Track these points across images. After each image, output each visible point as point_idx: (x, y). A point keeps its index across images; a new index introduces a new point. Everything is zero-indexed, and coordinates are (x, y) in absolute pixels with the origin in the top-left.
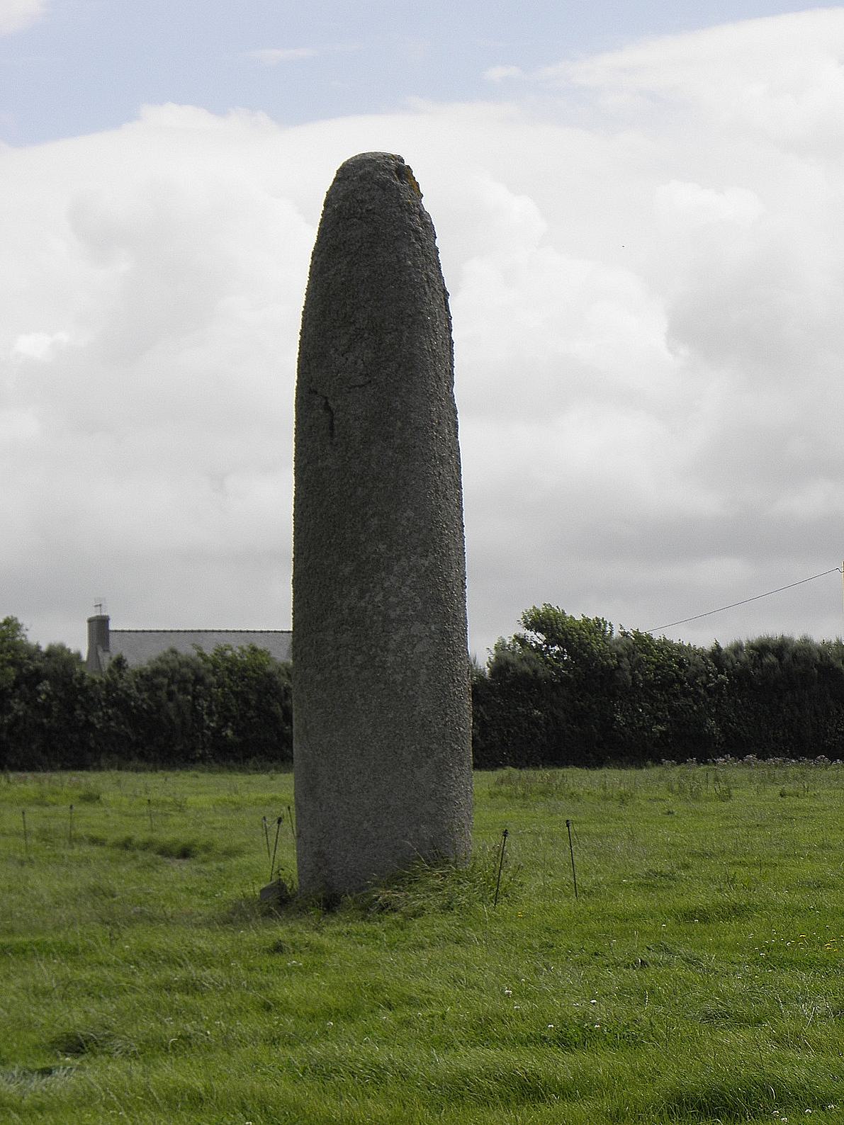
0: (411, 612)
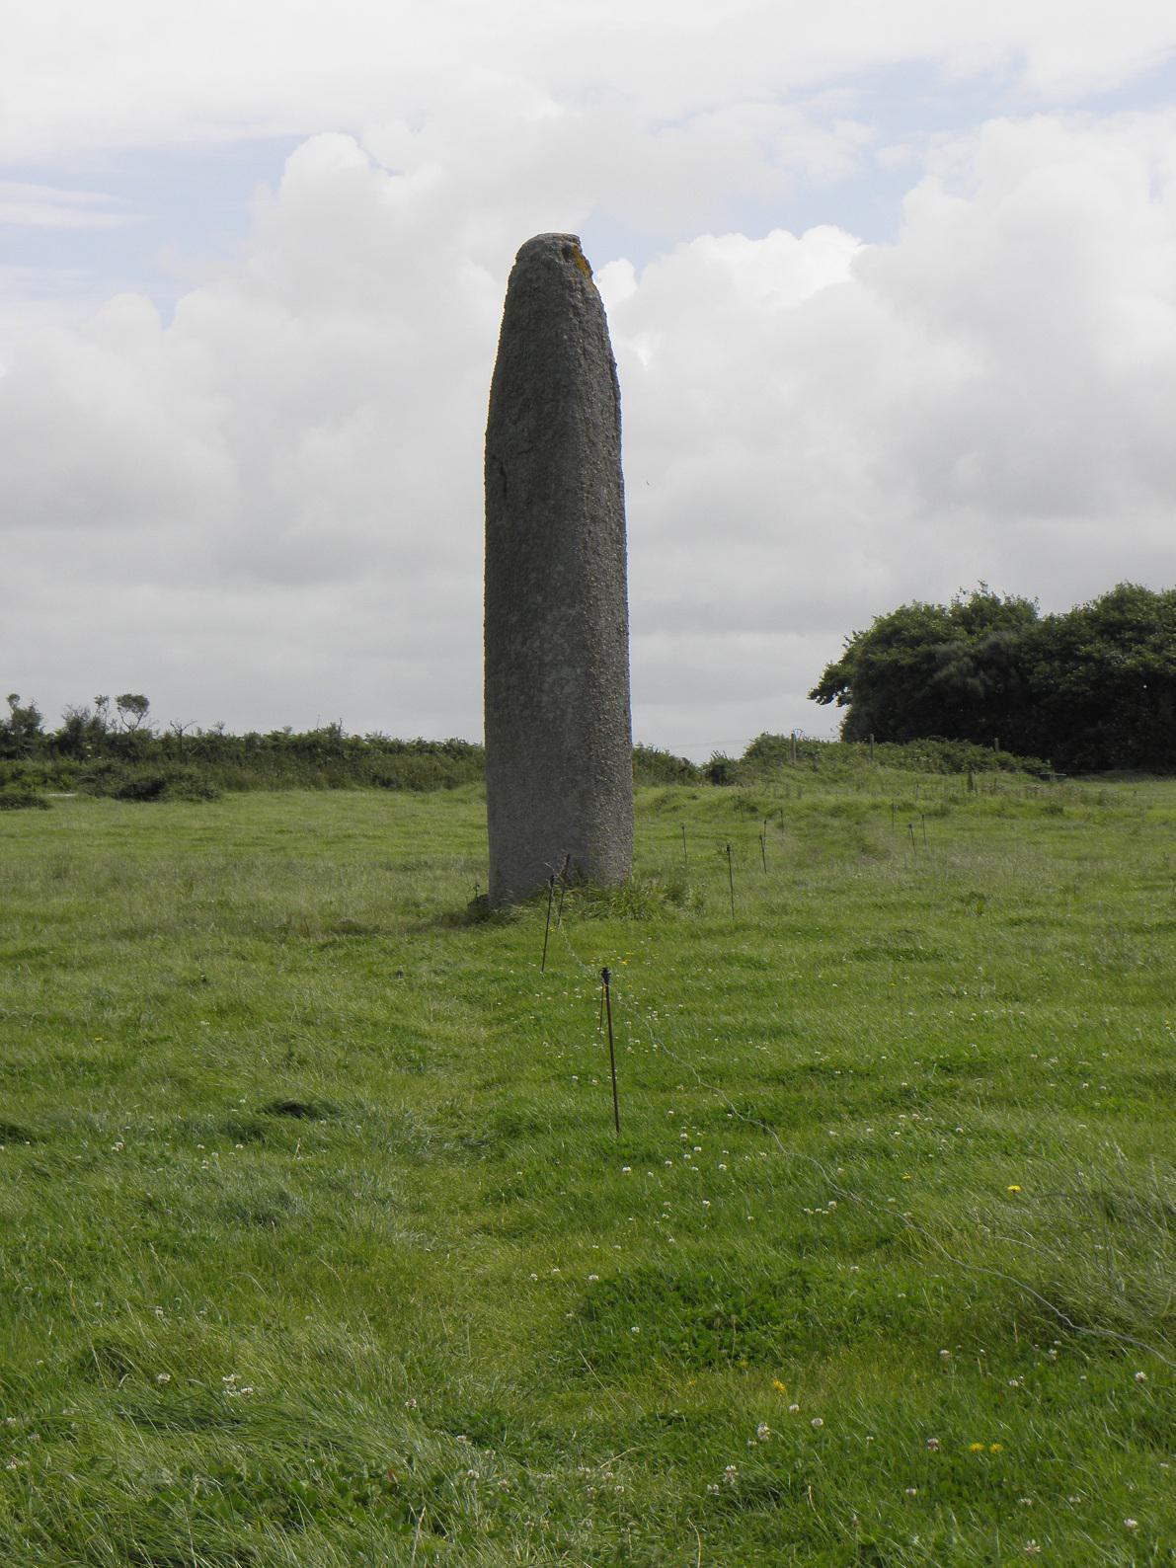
0: (560, 657)
